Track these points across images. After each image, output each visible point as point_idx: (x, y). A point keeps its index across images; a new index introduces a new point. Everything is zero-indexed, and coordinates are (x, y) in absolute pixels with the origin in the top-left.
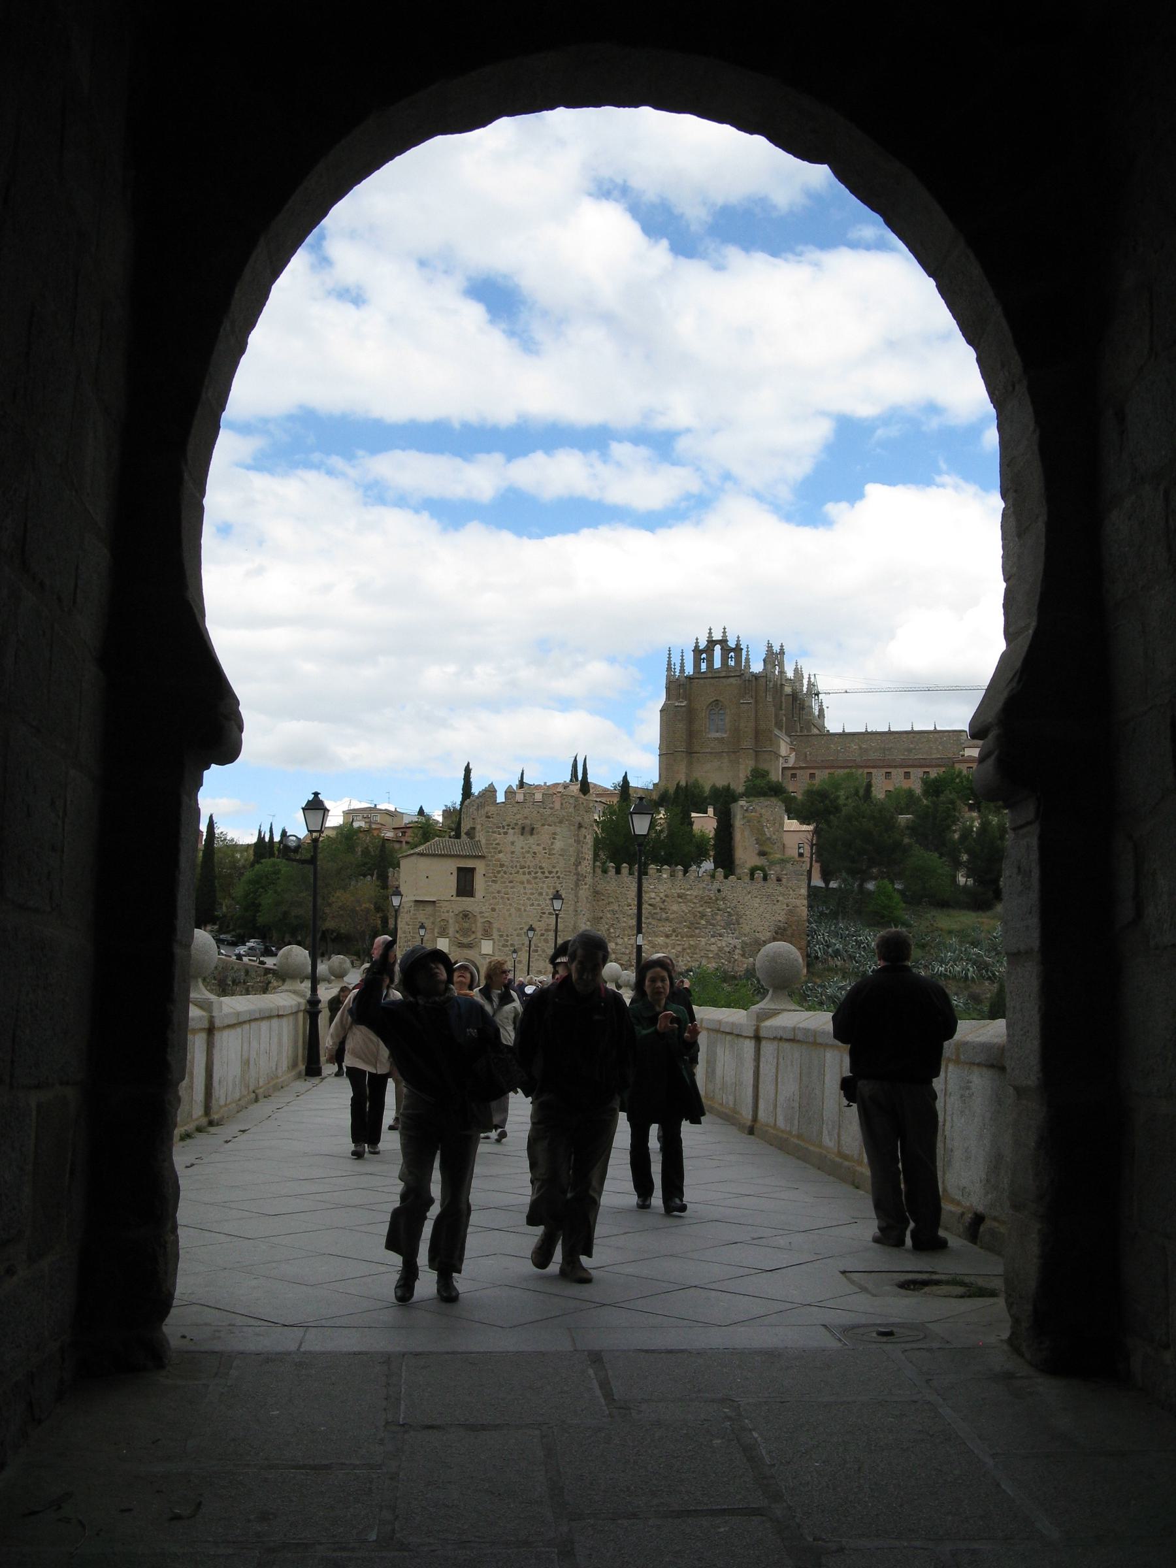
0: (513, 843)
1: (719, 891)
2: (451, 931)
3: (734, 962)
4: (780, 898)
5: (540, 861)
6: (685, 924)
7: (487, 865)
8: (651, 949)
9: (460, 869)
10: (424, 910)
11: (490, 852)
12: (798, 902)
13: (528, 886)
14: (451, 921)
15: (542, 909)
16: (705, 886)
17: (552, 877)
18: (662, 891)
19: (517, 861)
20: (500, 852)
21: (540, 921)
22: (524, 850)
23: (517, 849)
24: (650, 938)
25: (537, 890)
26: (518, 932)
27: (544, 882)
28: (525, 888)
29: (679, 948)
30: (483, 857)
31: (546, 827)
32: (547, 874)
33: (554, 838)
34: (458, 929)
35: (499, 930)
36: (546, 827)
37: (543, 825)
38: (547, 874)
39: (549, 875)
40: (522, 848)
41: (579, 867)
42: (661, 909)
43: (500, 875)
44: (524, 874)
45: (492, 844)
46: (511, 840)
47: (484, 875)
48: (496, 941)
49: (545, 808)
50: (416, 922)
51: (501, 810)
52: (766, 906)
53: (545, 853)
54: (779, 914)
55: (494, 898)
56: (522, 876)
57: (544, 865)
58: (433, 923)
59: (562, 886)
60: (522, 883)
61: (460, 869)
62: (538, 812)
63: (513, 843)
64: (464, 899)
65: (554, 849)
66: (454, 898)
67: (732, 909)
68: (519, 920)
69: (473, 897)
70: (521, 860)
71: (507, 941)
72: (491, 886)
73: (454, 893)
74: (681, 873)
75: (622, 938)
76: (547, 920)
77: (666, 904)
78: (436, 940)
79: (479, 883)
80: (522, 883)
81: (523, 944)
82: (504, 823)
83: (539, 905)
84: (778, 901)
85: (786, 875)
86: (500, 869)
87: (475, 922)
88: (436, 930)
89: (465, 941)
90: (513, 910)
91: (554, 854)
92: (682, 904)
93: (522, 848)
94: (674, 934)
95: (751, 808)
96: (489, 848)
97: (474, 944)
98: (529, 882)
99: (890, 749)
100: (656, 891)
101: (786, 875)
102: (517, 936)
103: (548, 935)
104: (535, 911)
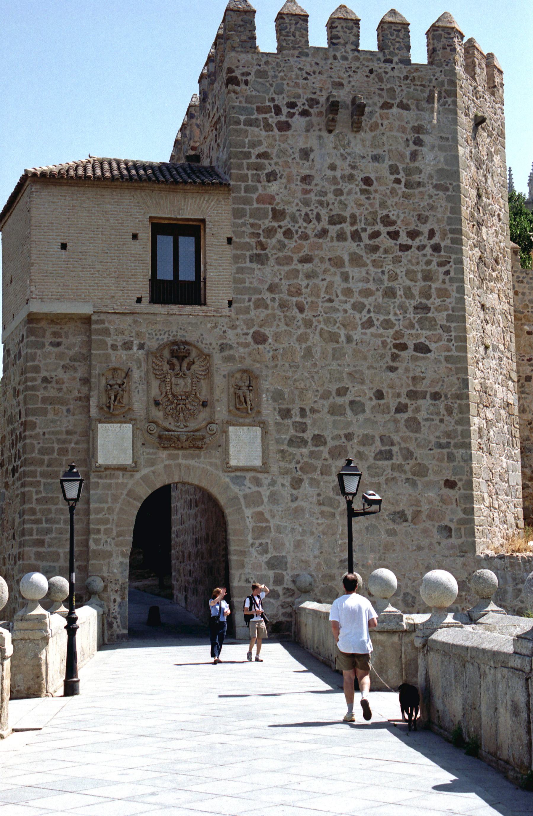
0: (305, 154)
5: (383, 205)
7: (238, 214)
10: (59, 344)
13: (355, 272)
14: (136, 374)
15: (398, 335)
17: (419, 248)
19: (321, 203)
20: (272, 176)
21: (392, 369)
22: (338, 173)
25: (381, 281)
26: (331, 400)
27: (397, 260)
28: (346, 277)
31: (395, 110)
32: (403, 239)
33: (418, 142)
36: (395, 110)
37: (386, 106)
39: (410, 242)
40: (333, 167)
41: (484, 229)
43: (274, 241)
44: (341, 237)
45: (247, 155)
46: (301, 144)
47: (229, 241)
48: (272, 428)
49: (390, 61)
50: (34, 379)
51: (267, 63)
55: (260, 304)
56: (335, 243)
58: (86, 381)
59: (447, 273)
60: (337, 262)
62: (371, 72)
63: (305, 154)
64: (174, 308)
65: (420, 171)
66: (145, 306)
69: (200, 304)
70: (331, 197)
71: (303, 427)
76: (411, 366)
81: (349, 437)
83: (387, 324)
86: (276, 224)
87: (208, 374)
88: (93, 402)
90: (315, 338)
91: (419, 184)
93: (333, 167)
98: (356, 260)
103: (417, 410)
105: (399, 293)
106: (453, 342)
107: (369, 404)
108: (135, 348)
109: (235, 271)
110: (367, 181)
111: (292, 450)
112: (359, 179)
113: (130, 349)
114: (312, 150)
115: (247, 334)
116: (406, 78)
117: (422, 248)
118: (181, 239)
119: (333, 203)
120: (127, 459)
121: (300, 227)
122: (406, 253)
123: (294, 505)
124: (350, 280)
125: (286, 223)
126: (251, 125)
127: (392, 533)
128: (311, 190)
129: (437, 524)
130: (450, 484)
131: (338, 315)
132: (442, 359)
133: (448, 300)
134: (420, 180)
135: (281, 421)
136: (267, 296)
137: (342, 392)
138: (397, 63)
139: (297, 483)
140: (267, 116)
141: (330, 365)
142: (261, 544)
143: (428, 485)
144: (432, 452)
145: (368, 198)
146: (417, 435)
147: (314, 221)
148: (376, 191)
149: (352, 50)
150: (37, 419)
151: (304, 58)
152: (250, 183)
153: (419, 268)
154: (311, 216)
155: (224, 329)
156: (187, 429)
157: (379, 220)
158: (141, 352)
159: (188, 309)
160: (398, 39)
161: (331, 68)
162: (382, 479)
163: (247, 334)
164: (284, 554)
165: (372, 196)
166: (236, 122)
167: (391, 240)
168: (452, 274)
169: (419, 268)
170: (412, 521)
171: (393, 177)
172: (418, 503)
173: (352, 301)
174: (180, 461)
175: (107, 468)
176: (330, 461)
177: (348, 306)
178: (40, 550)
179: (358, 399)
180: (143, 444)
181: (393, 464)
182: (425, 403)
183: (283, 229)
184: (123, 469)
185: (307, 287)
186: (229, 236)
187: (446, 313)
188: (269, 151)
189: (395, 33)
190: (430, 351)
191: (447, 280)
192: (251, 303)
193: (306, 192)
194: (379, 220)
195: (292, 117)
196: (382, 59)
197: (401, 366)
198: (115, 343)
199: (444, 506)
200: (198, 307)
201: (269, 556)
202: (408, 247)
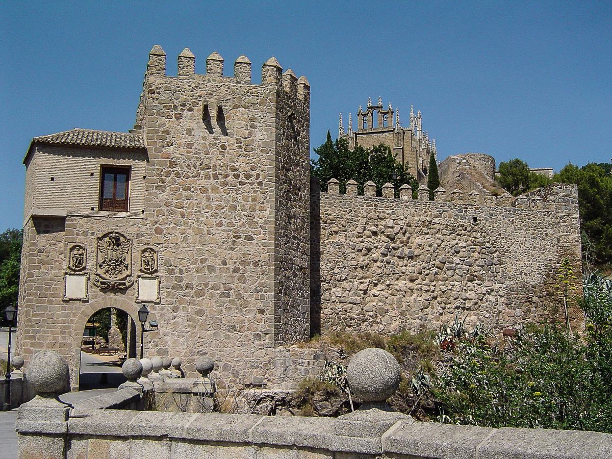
0: (189, 131)
1: (475, 219)
2: (90, 263)
3: (498, 314)
4: (549, 231)
6: (434, 262)
8: (391, 297)
9: (105, 169)
11: (155, 144)
13: (213, 196)
16: (457, 213)
18: (402, 217)
19: (197, 158)
21: (232, 249)
22: (207, 143)
24: (388, 282)
25: (228, 201)
28: (208, 198)
29: (426, 296)
31: (241, 109)
32: (242, 178)
34: (101, 260)
35: (168, 264)
36: (241, 109)
37: (236, 107)
39: (246, 181)
40: (204, 139)
42: (402, 242)
43: (170, 178)
44: (207, 177)
45: (157, 132)
47: (145, 177)
49: (240, 83)
52: (533, 240)
53: (240, 147)
54: (549, 251)
55: (161, 213)
57: (237, 165)
60: (204, 191)
61: (105, 169)
63: (189, 131)
66: (96, 212)
67: (492, 244)
68: (199, 247)
72: (156, 196)
73: (96, 204)
74: (426, 195)
75: (350, 281)
76: (243, 247)
77: (407, 235)
78: (65, 278)
79: (136, 189)
80: (204, 191)
81: (206, 285)
82: (176, 102)
84: (547, 235)
85: (554, 201)
86: (172, 170)
89: (112, 279)
92: (428, 236)
93: (204, 139)
94: (420, 276)
95: (465, 161)
96: (153, 138)
97: (128, 284)
98: (215, 190)
100: (394, 216)
101: (554, 201)
102: (197, 271)
104: (225, 234)
105: (238, 208)
106: (267, 235)
107: (217, 267)
108: (89, 235)
109: (147, 194)
110: (224, 147)
111: (173, 291)
112: (219, 146)
113: (86, 235)
114: (193, 130)
115: (152, 229)
116: (248, 92)
117: (252, 184)
118: (118, 176)
119: (204, 159)
120: (82, 295)
121: (184, 171)
122: (243, 186)
123: (173, 321)
124: (211, 200)
125: (178, 168)
126: (159, 115)
127: (228, 337)
128: (192, 152)
129: (253, 333)
130: (262, 311)
131: (203, 219)
132: (260, 244)
133: (265, 212)
134: (253, 147)
135: (169, 275)
136: (164, 208)
137: (202, 261)
138: (243, 84)
139: (175, 310)
140: (170, 111)
141: (197, 246)
142: (154, 342)
143: (250, 311)
144: (252, 294)
145: (224, 156)
146: (245, 285)
147: (193, 168)
148: (228, 153)
149: (219, 76)
150: (35, 272)
151: (192, 80)
152: (158, 147)
153: (250, 195)
154: (191, 166)
155: (139, 225)
156: (116, 279)
157: (229, 168)
158: (92, 237)
159: (119, 214)
160: (244, 71)
161: (206, 86)
162: (222, 308)
163: (152, 229)
164: (167, 347)
165: (226, 155)
166: (151, 113)
167: (235, 179)
168: (268, 198)
169: (250, 195)
170: (239, 331)
171: (237, 145)
172: (243, 321)
173: (213, 211)
174: (111, 296)
175: (70, 300)
176: (195, 298)
177: (209, 214)
178: (33, 341)
179: (211, 264)
180: (91, 287)
181: (230, 300)
182: (250, 267)
183: (175, 172)
184: (79, 300)
185: (186, 204)
186: (144, 175)
187: (264, 219)
188: (170, 130)
189: (243, 68)
190: (254, 240)
191: (265, 202)
192: (155, 212)
193: (188, 152)
194: (229, 168)
195: (183, 112)
196: (235, 82)
197: (238, 247)
198: (78, 232)
199: (257, 323)
200: (125, 213)
201: (158, 348)
202: (244, 183)
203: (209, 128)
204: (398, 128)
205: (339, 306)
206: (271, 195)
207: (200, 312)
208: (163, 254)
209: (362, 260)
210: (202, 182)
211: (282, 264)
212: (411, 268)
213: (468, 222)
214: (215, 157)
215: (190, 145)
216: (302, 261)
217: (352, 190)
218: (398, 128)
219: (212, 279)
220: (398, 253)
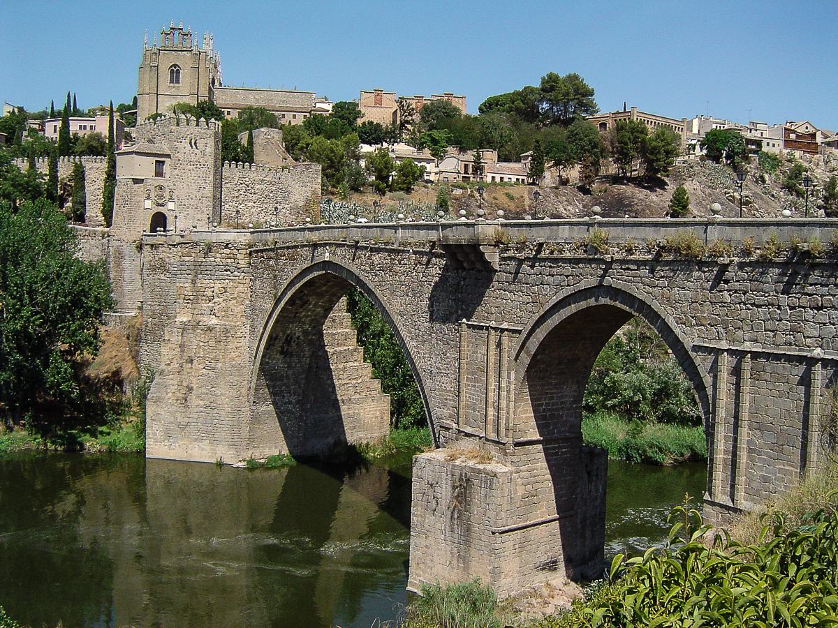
2: (153, 195)
9: (157, 161)
12: (317, 186)
20: (178, 152)
23: (187, 152)
29: (259, 209)
30: (168, 156)
32: (202, 166)
38: (202, 166)
61: (157, 161)
63: (185, 148)
79: (166, 168)
99: (272, 100)
203: (192, 147)
204: (195, 50)
205: (228, 212)
206: (212, 172)
207: (188, 214)
208: (176, 193)
209: (237, 194)
210: (188, 167)
211: (214, 196)
212: (254, 197)
213: (277, 180)
214: (193, 158)
215: (185, 153)
216: (218, 196)
217: (233, 166)
218: (195, 50)
219: (192, 202)
220: (250, 192)
